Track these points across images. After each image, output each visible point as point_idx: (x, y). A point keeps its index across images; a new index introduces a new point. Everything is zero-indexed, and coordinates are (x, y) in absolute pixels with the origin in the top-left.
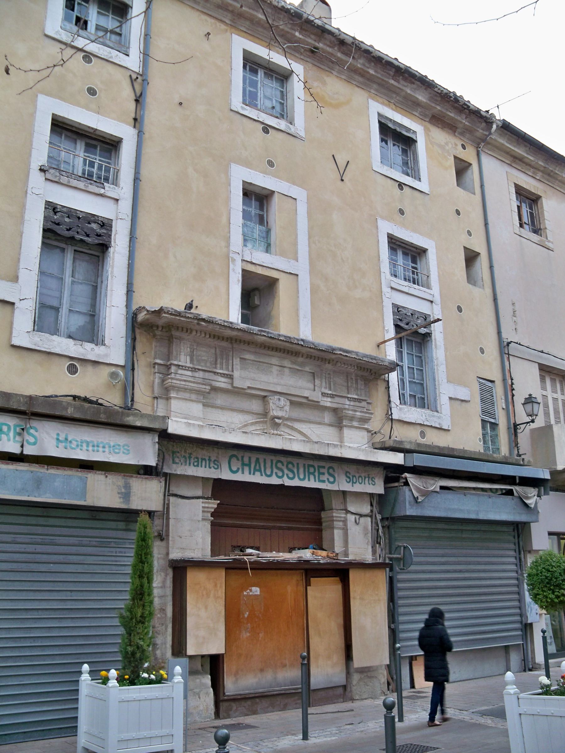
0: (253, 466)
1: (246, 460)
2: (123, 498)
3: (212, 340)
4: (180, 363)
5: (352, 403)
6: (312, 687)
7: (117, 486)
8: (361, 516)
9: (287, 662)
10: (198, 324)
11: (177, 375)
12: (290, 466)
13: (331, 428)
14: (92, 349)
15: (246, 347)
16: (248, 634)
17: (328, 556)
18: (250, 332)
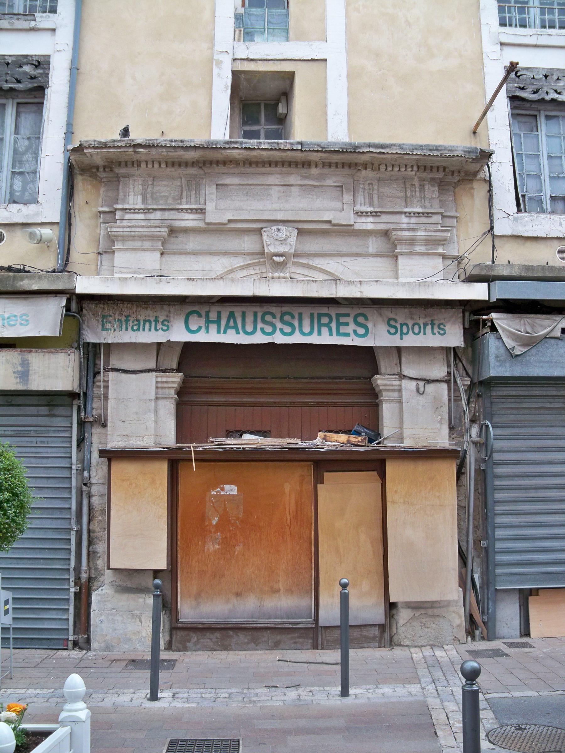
0: (223, 323)
1: (213, 316)
2: (20, 378)
3: (173, 169)
4: (126, 206)
5: (413, 220)
6: (351, 622)
7: (13, 364)
8: (428, 381)
9: (281, 587)
10: (135, 152)
11: (124, 221)
12: (287, 318)
13: (379, 259)
14: (19, 210)
15: (221, 169)
16: (217, 547)
17: (349, 441)
18: (212, 148)
